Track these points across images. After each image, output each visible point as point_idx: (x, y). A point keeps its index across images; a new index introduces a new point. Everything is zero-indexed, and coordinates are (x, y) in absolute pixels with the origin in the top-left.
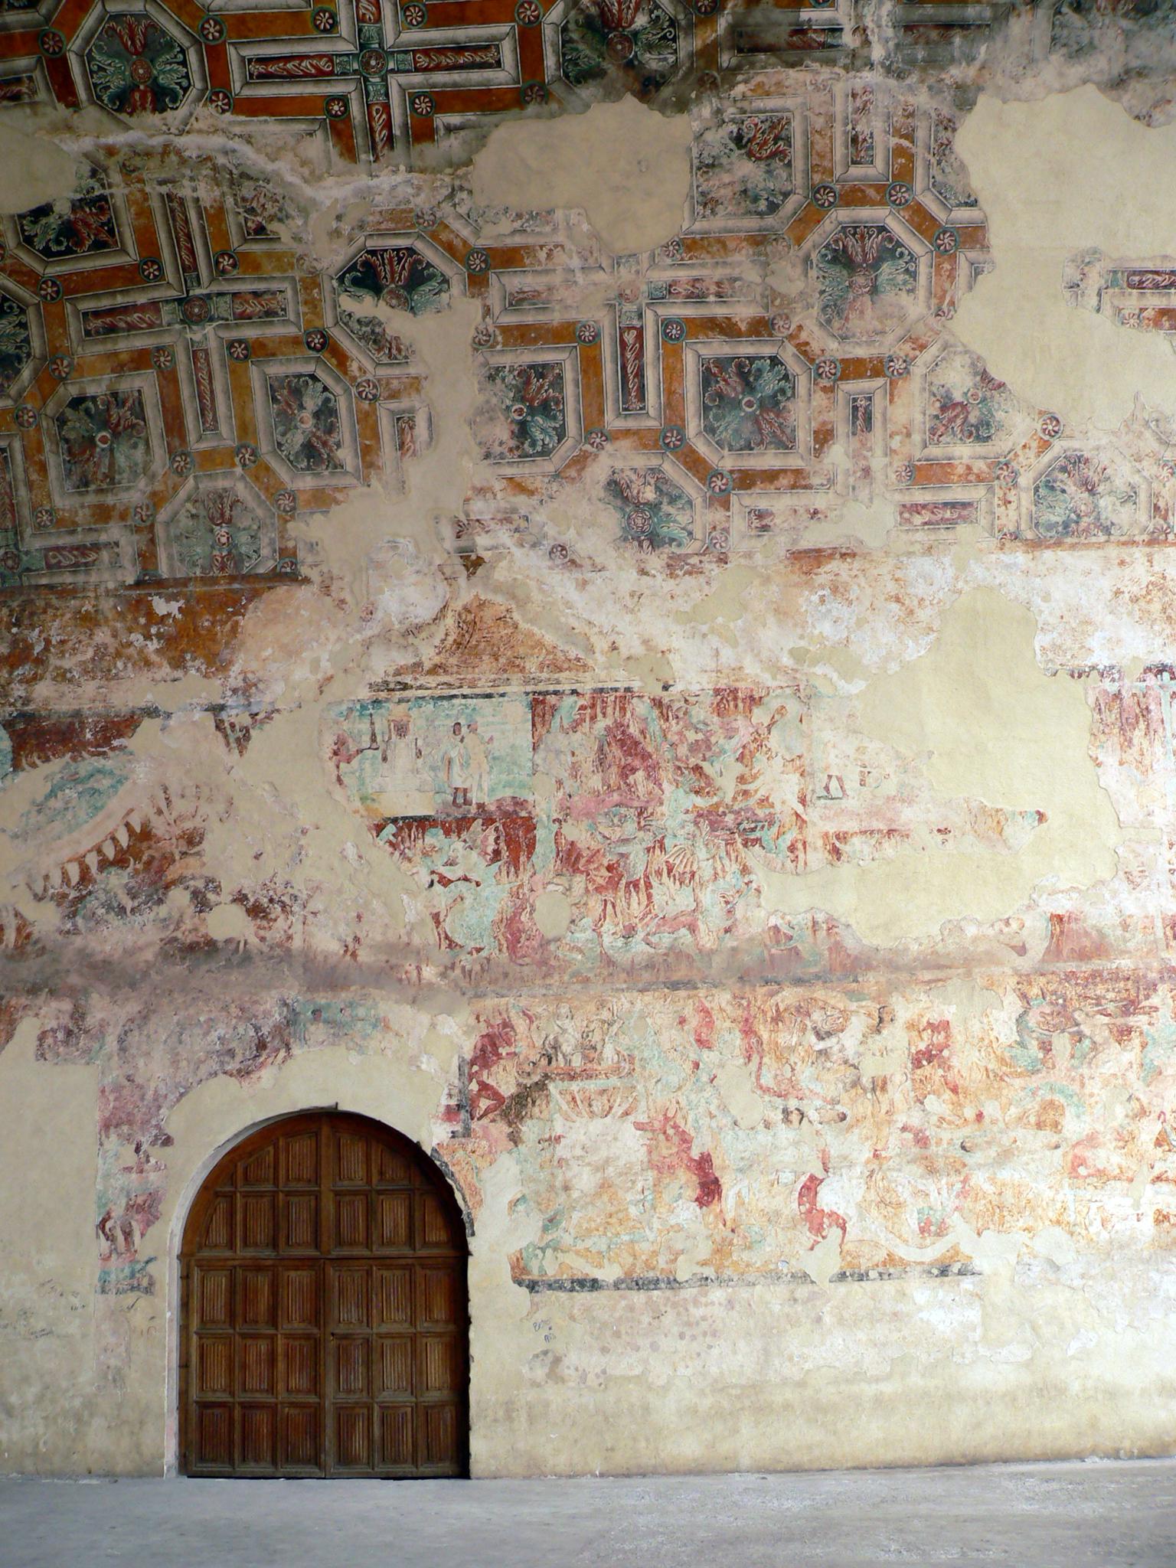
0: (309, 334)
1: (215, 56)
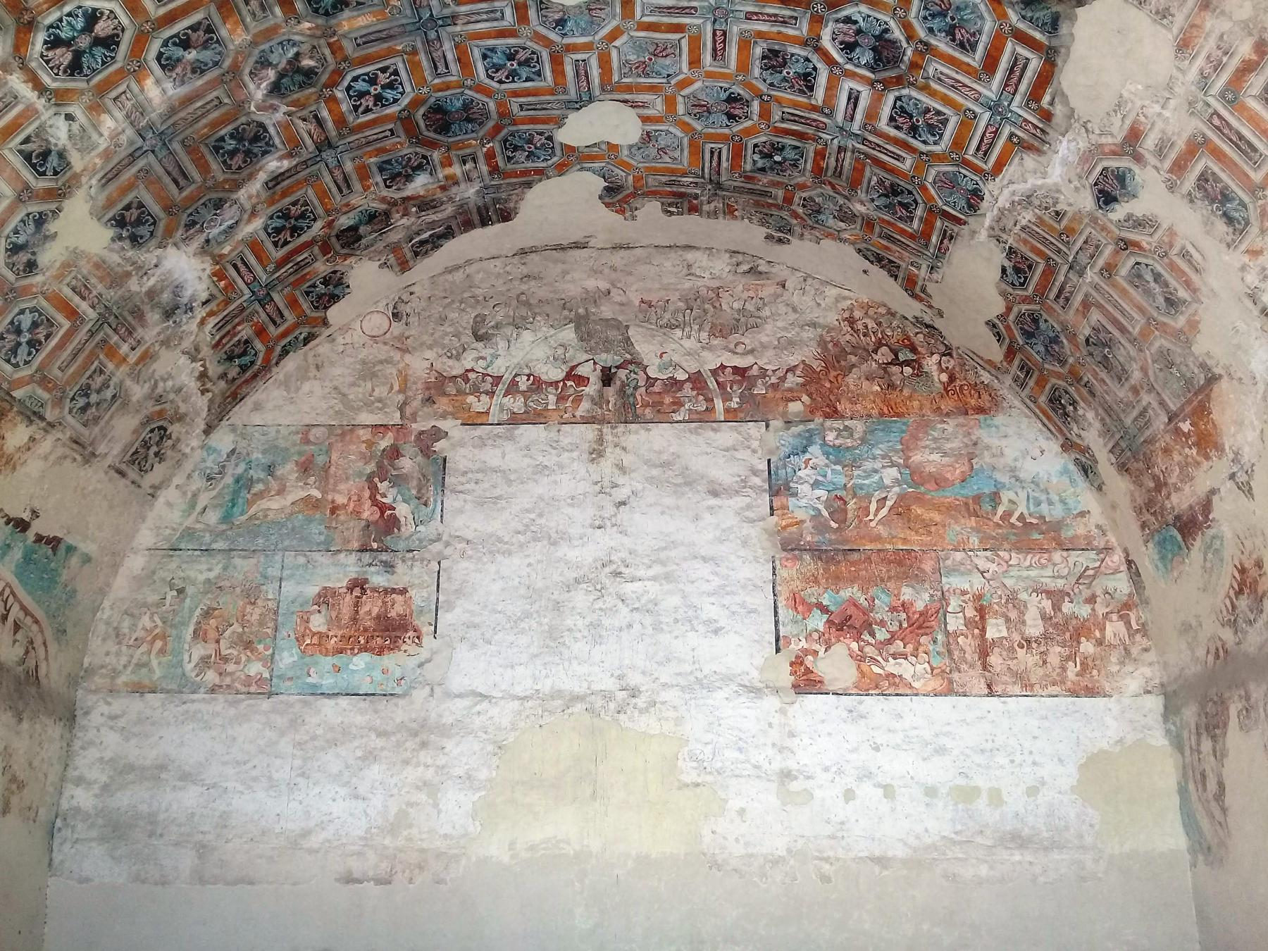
0: (1117, 244)
1: (966, 163)
